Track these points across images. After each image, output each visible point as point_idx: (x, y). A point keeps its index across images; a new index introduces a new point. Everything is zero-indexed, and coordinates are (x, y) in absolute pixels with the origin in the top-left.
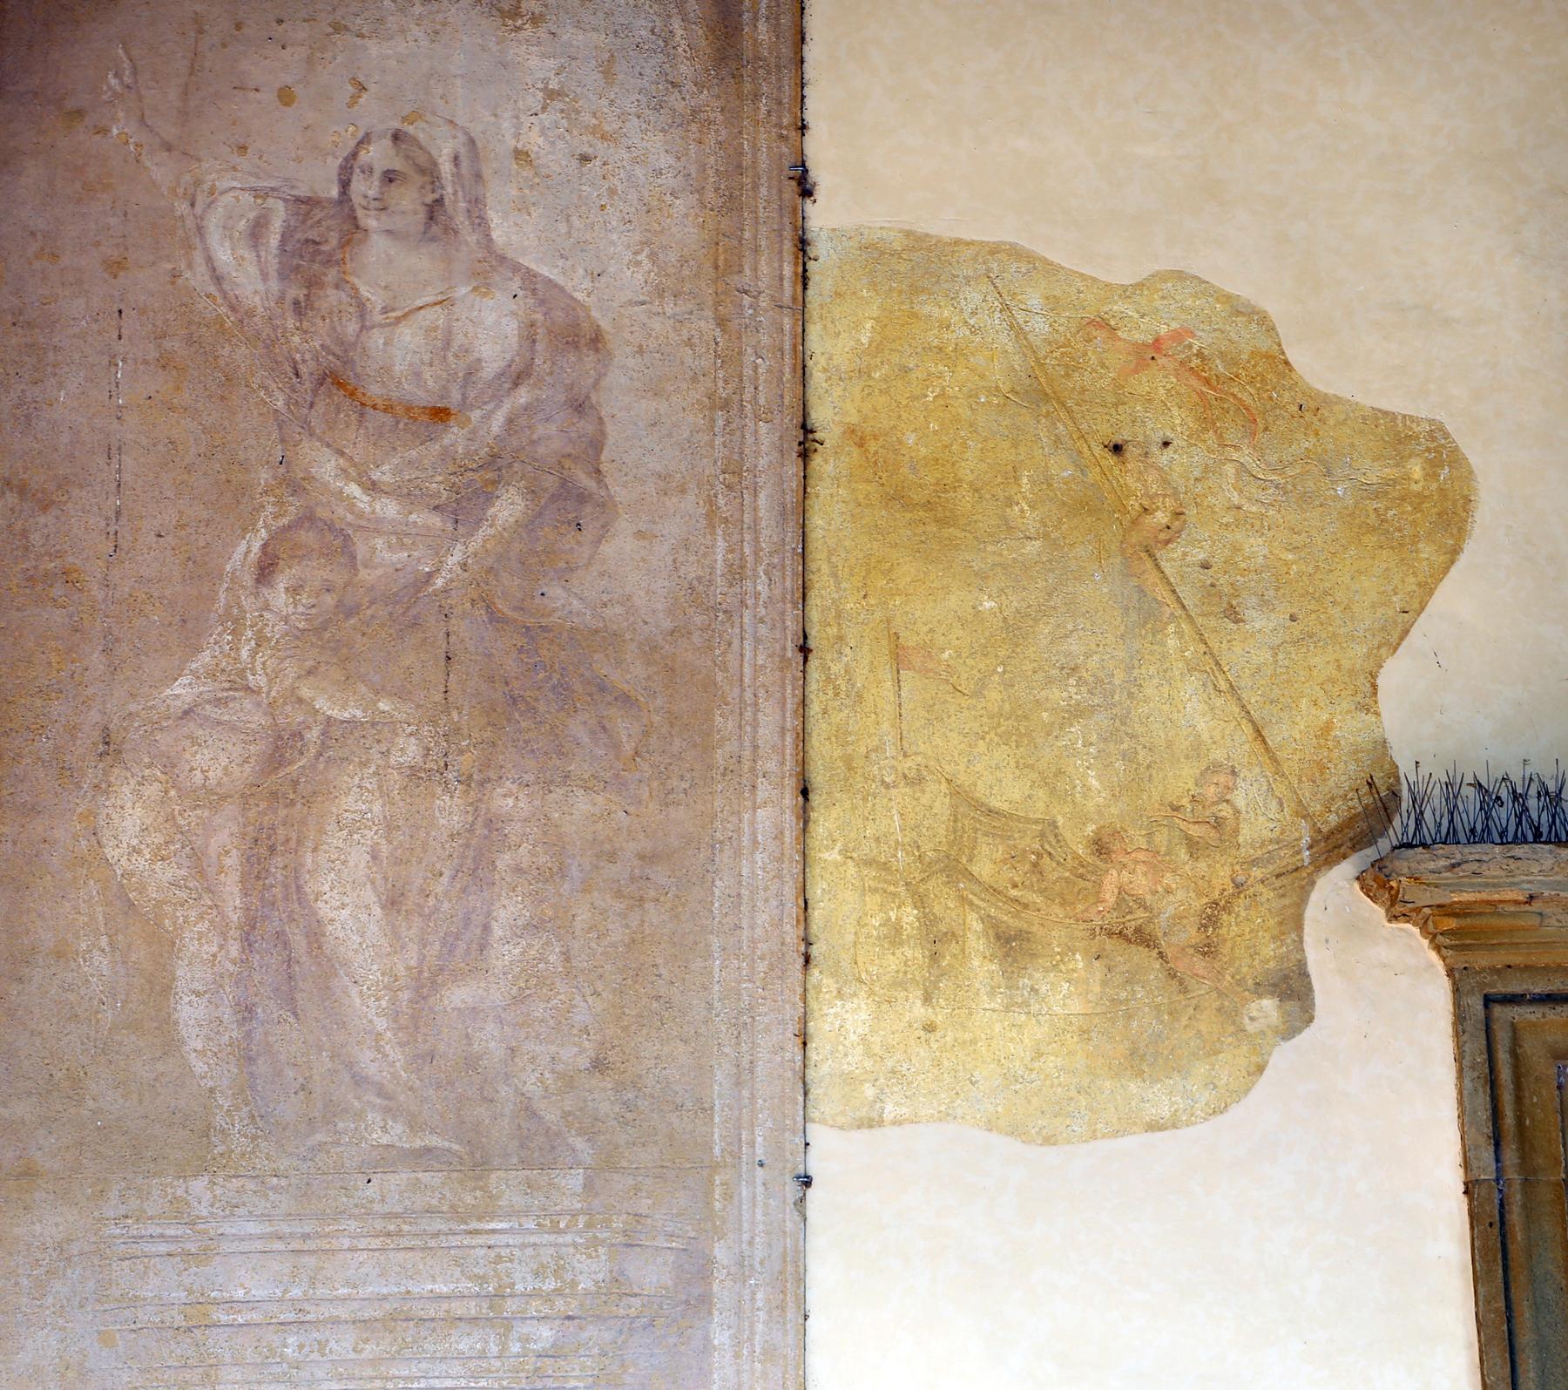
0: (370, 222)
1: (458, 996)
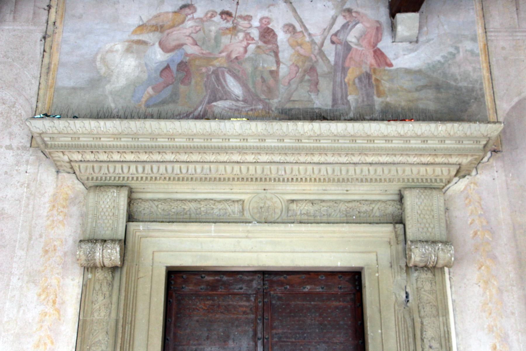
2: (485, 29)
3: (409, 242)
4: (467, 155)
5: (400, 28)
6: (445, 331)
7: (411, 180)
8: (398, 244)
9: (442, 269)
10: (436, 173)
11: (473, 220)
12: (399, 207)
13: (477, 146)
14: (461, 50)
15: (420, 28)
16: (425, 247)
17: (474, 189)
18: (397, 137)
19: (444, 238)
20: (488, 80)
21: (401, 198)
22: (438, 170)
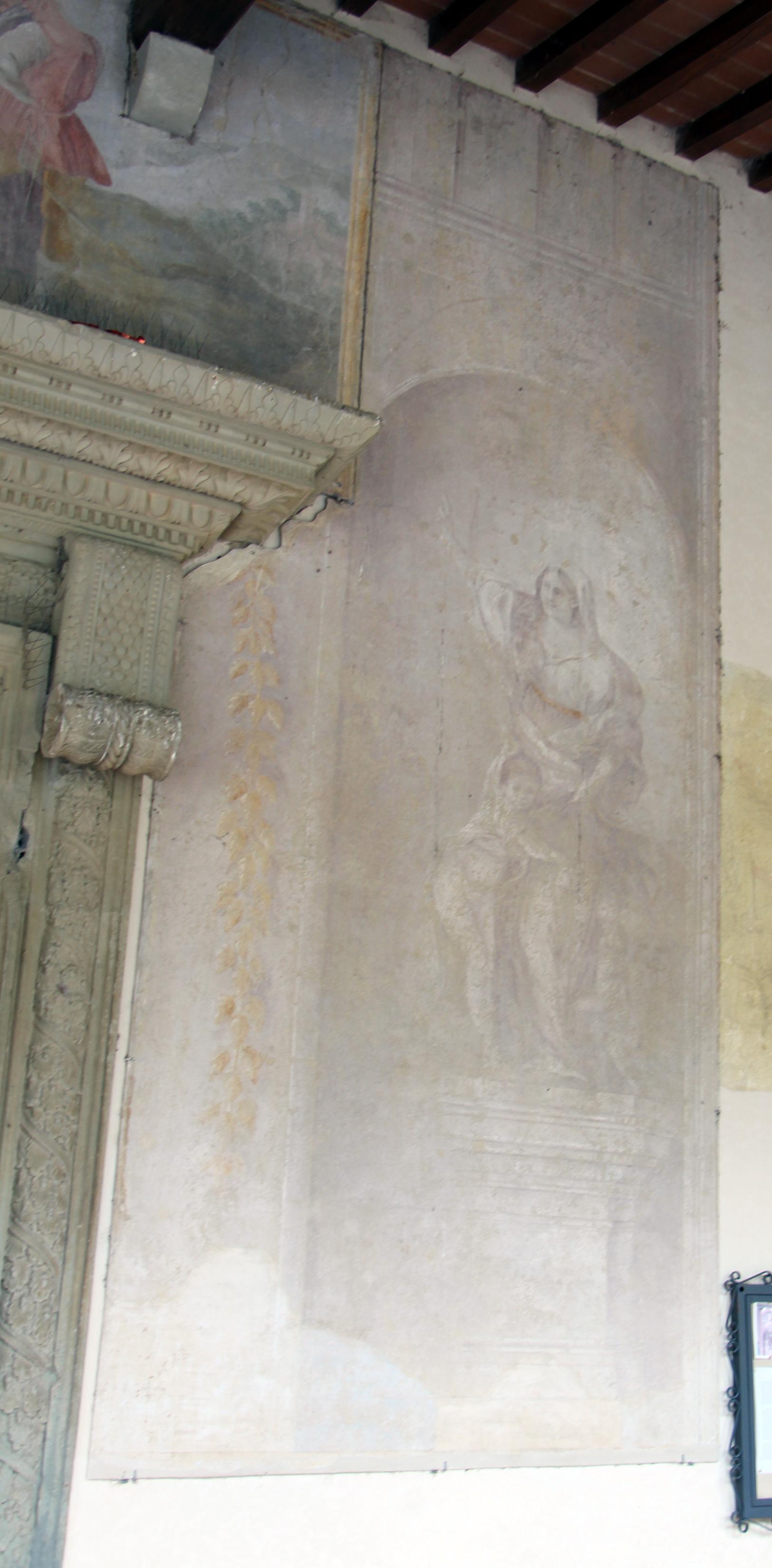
0: (549, 611)
1: (584, 1004)
2: (375, 171)
3: (59, 689)
4: (267, 483)
5: (151, 80)
6: (108, 952)
7: (98, 517)
8: (25, 687)
9: (136, 779)
10: (174, 514)
11: (244, 667)
12: (49, 584)
13: (301, 465)
14: (303, 204)
15: (208, 104)
16: (102, 710)
17: (262, 585)
18: (87, 378)
19: (160, 697)
20: (357, 307)
21: (60, 562)
22: (181, 506)
